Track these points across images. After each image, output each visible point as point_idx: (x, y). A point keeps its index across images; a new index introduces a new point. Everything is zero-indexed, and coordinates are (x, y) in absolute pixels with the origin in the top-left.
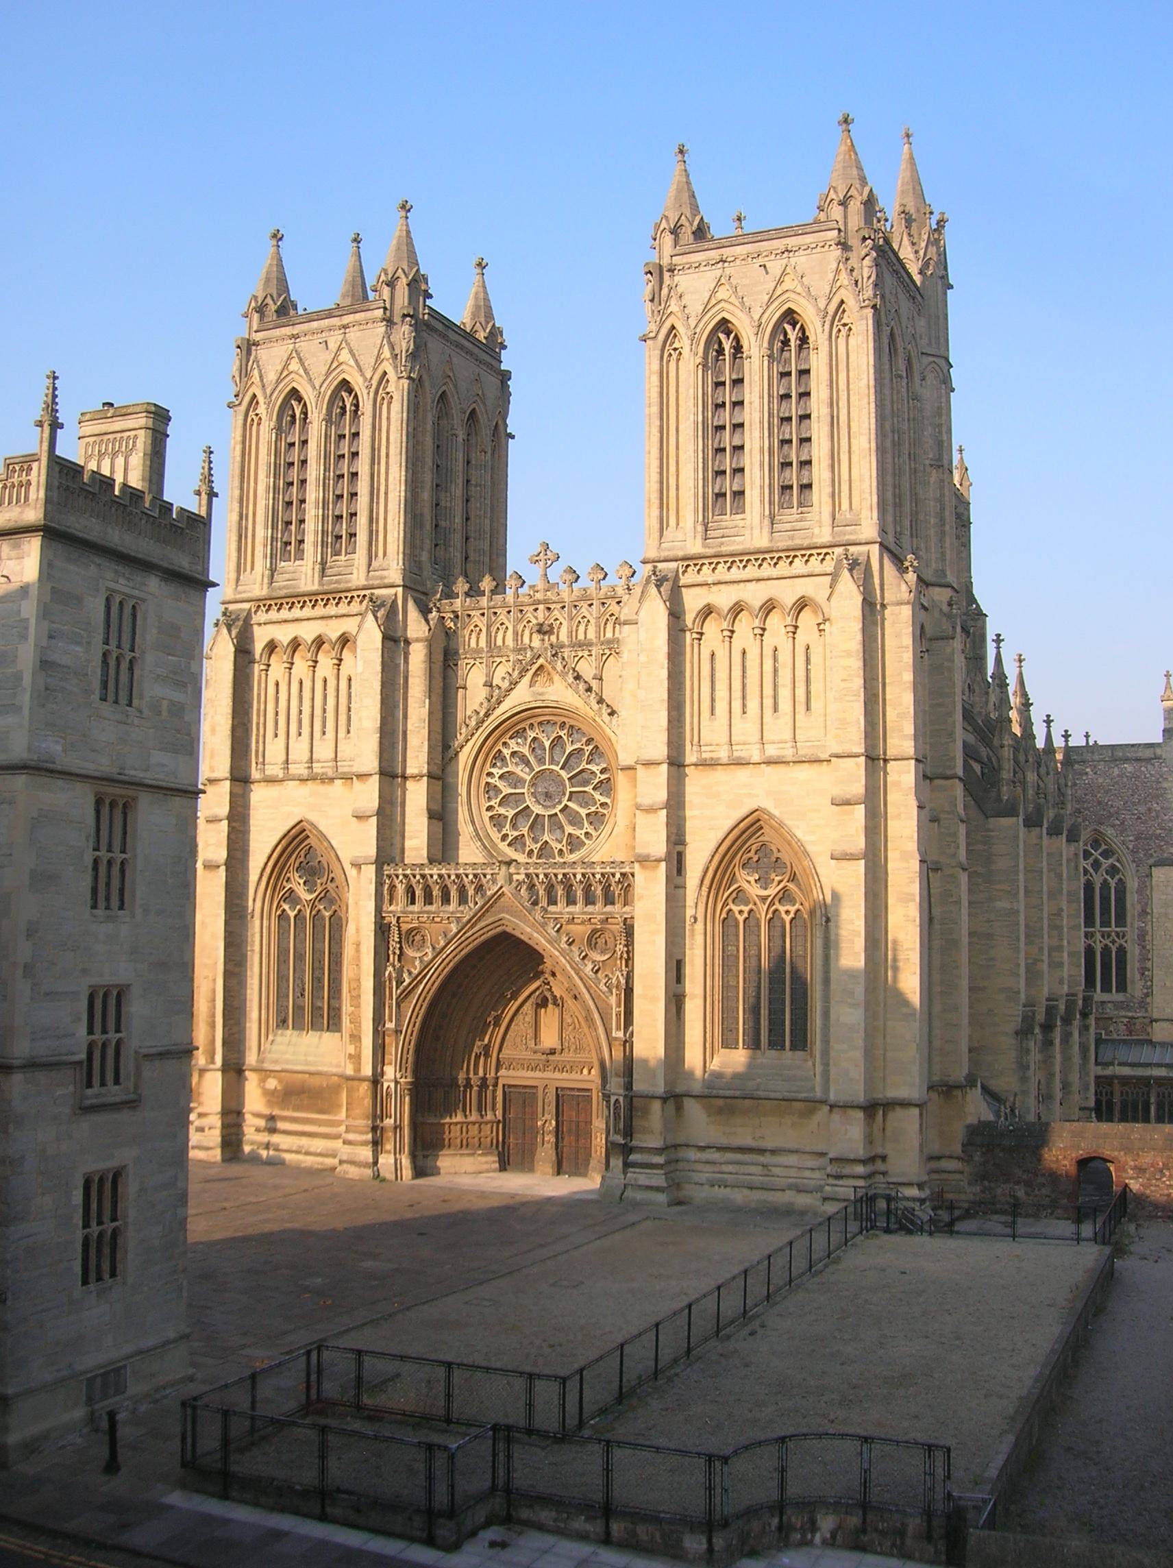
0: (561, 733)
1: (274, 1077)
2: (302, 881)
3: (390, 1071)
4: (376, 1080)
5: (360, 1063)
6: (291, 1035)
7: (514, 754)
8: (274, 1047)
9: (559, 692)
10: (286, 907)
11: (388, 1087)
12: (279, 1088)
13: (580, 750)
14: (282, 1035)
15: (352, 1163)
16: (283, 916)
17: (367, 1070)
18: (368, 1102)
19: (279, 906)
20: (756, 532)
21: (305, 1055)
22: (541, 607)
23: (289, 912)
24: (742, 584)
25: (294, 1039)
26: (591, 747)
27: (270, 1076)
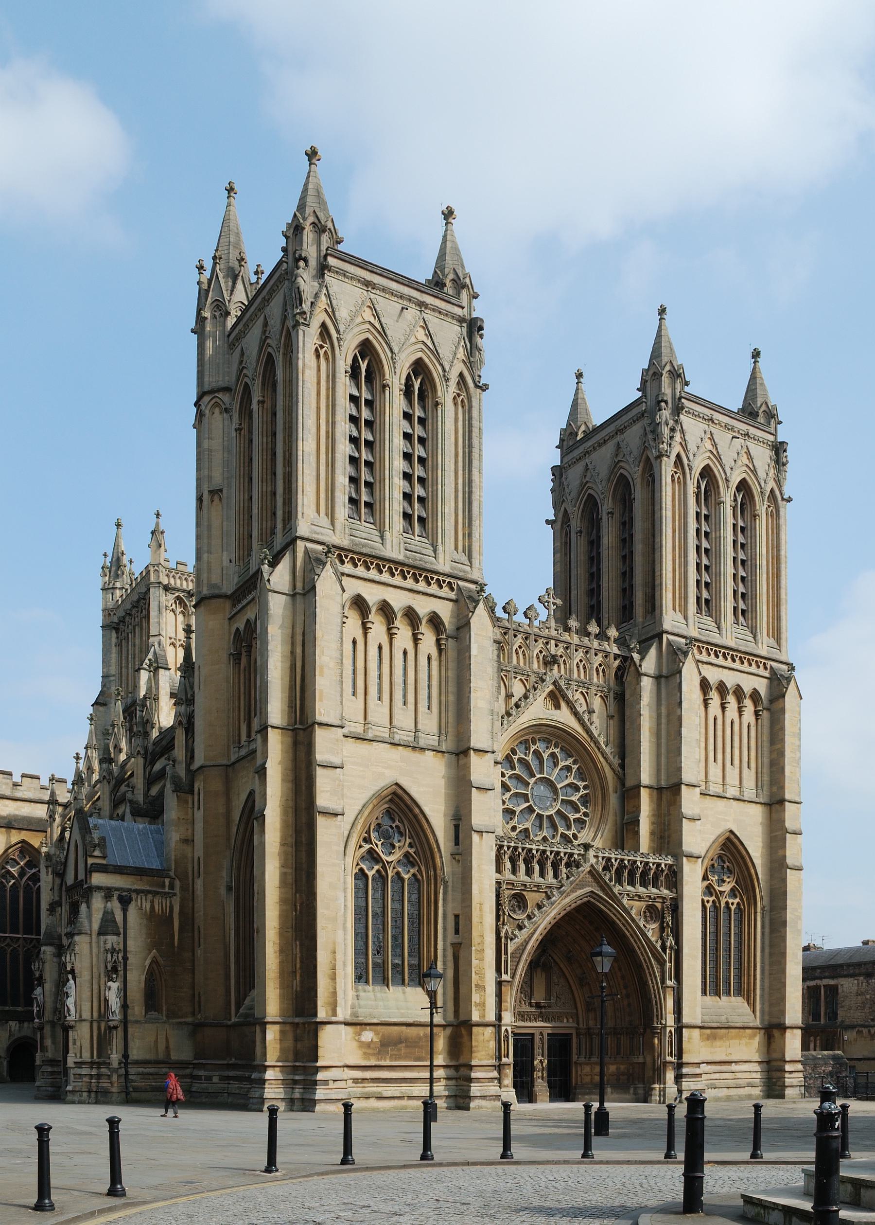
0: (556, 751)
1: (370, 1030)
2: (379, 843)
3: (508, 1018)
4: (497, 1025)
5: (484, 1010)
6: (373, 991)
7: (519, 760)
8: (362, 1002)
9: (564, 717)
10: (364, 867)
11: (506, 1030)
12: (376, 1040)
13: (568, 768)
14: (365, 991)
15: (483, 1097)
16: (361, 875)
17: (491, 1017)
18: (492, 1044)
19: (358, 865)
20: (729, 633)
21: (398, 1009)
22: (553, 642)
23: (367, 871)
24: (721, 669)
25: (379, 995)
26: (576, 767)
27: (365, 1030)
